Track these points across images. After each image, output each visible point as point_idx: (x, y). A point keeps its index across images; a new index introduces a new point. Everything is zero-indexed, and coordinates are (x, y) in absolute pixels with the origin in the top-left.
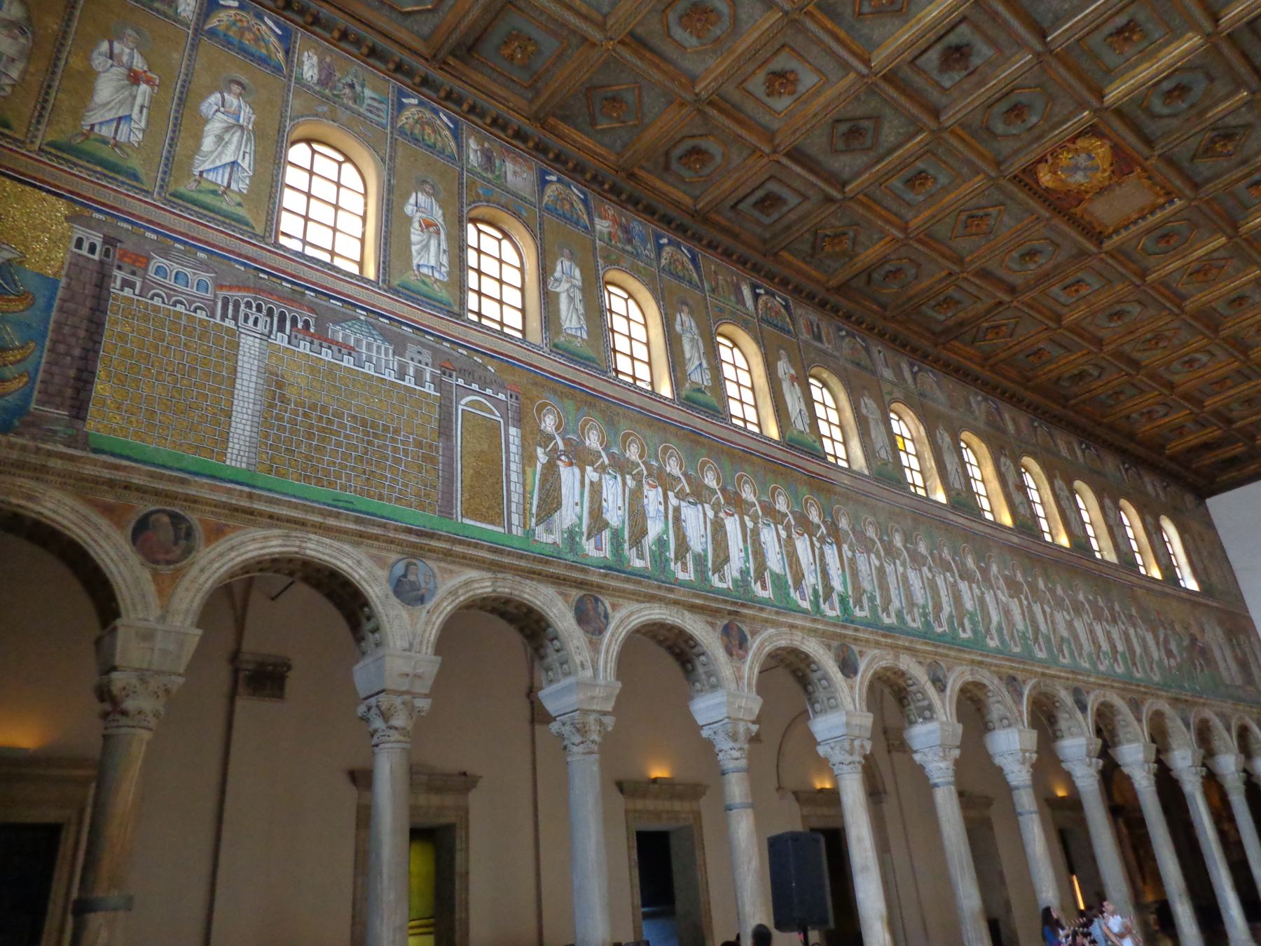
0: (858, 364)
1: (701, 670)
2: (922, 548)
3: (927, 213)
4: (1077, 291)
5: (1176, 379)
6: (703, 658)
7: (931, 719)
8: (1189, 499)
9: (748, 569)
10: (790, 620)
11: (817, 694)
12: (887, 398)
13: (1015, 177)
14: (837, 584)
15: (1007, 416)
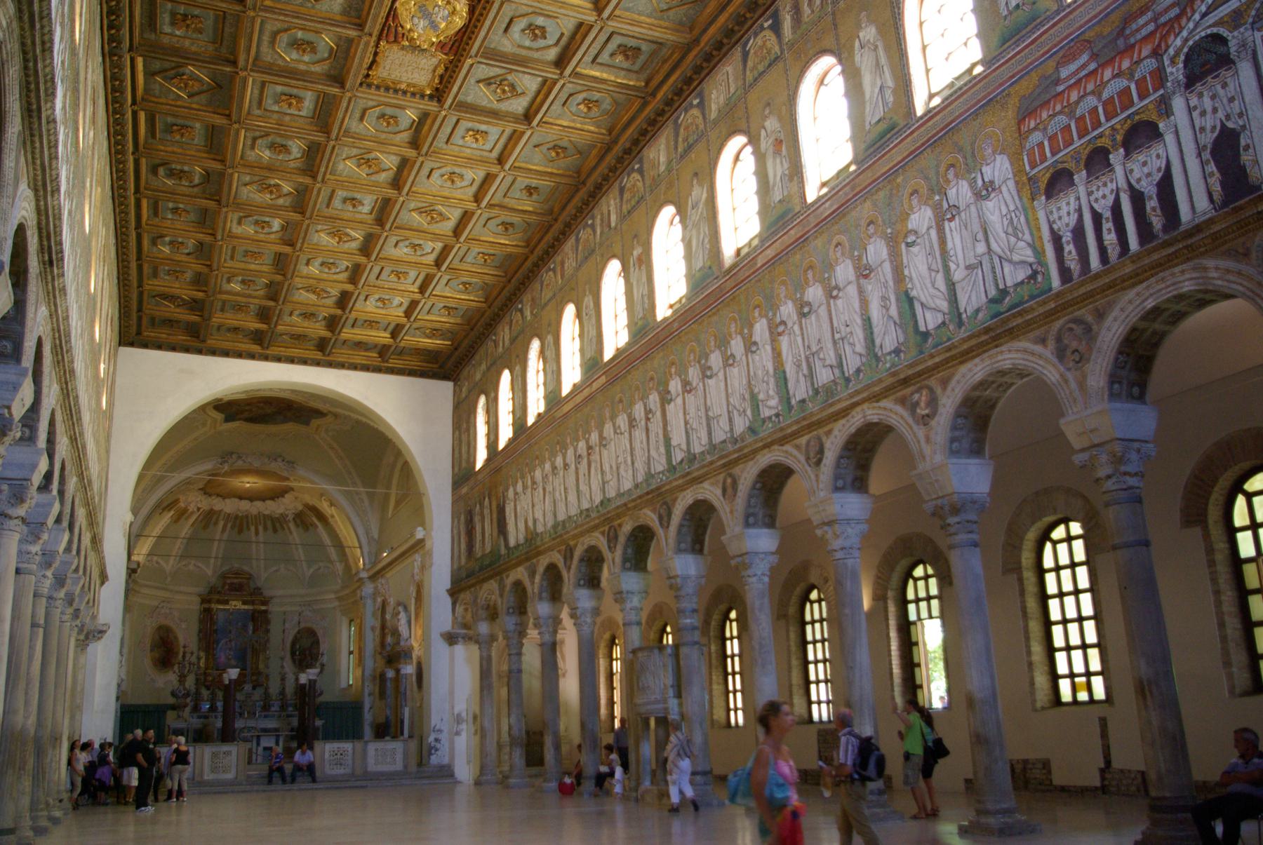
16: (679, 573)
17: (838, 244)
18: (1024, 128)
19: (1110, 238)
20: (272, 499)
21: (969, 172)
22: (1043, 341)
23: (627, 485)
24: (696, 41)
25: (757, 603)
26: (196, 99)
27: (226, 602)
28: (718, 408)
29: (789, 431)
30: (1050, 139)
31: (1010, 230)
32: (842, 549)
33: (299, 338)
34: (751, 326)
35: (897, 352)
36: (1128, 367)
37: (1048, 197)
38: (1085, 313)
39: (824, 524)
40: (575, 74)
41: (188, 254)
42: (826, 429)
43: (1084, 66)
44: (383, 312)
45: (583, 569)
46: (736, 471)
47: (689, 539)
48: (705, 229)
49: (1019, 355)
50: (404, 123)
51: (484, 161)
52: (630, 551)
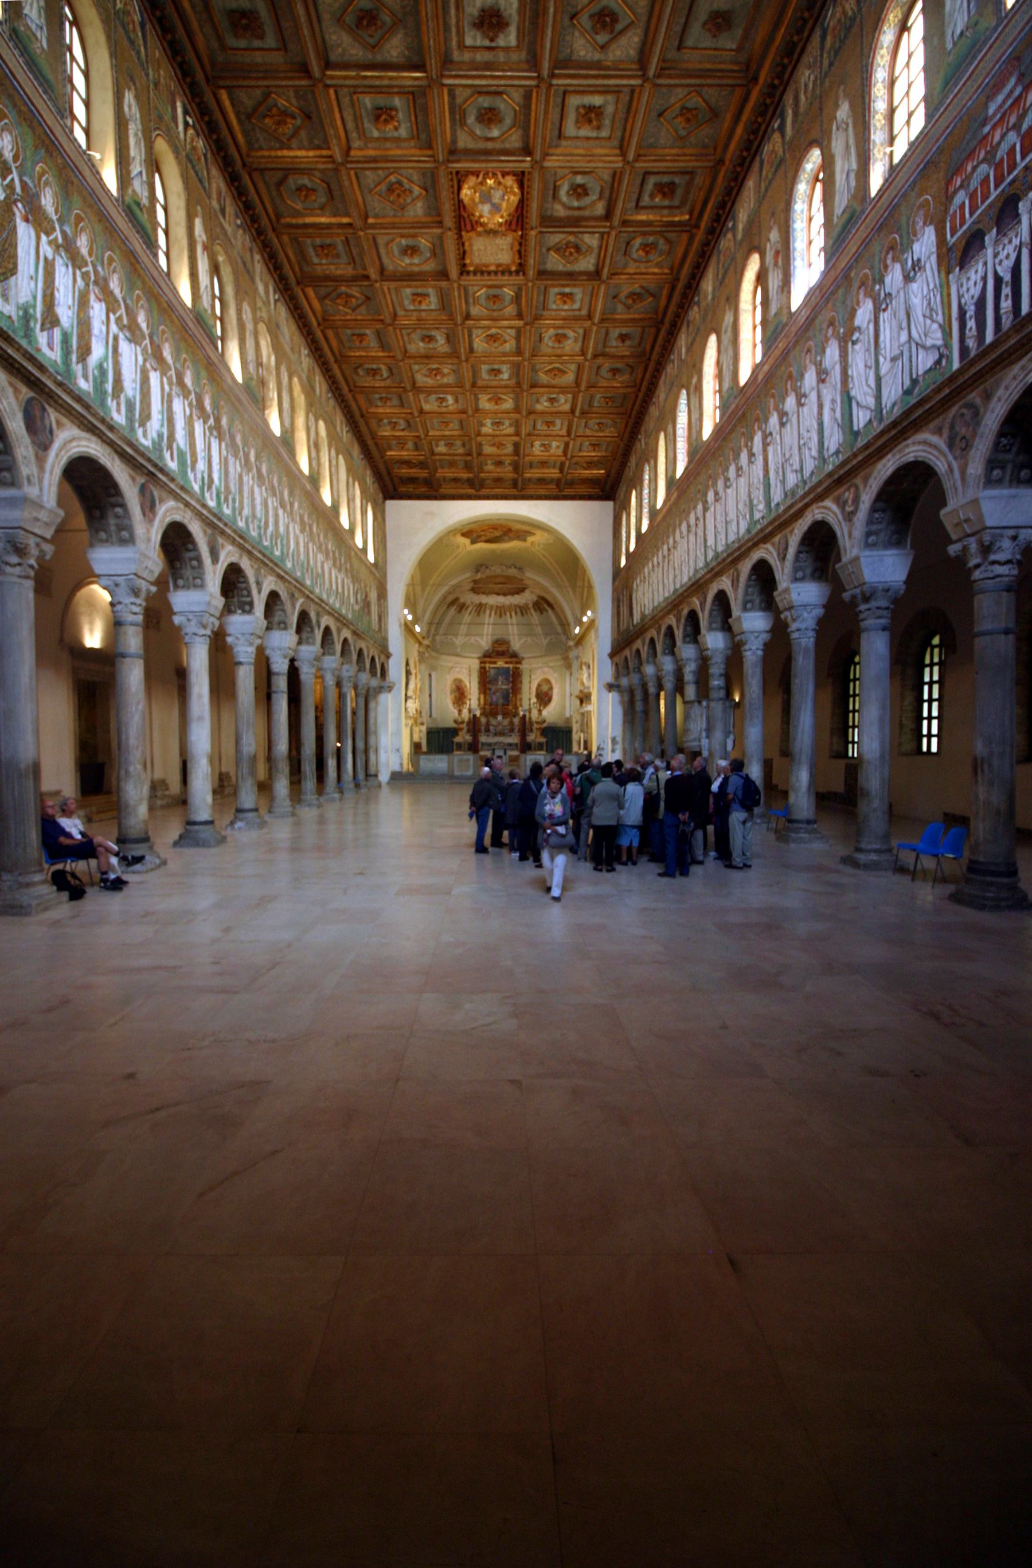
0: (244, 264)
1: (112, 521)
2: (264, 470)
3: (371, 153)
4: (420, 302)
5: (427, 407)
6: (119, 510)
7: (250, 612)
8: (381, 495)
9: (163, 434)
10: (188, 499)
11: (183, 572)
12: (259, 314)
13: (451, 173)
14: (216, 476)
15: (317, 378)
16: (709, 646)
17: (809, 350)
18: (951, 189)
19: (1006, 304)
20: (517, 593)
21: (903, 252)
22: (939, 431)
23: (685, 579)
24: (721, 162)
25: (750, 672)
26: (358, 311)
27: (495, 663)
28: (732, 516)
29: (767, 531)
30: (972, 197)
31: (928, 314)
32: (798, 630)
33: (498, 480)
34: (752, 439)
35: (837, 453)
36: (1015, 449)
37: (961, 270)
38: (974, 397)
39: (786, 609)
40: (625, 223)
41: (403, 430)
42: (791, 528)
43: (1011, 92)
44: (546, 454)
45: (667, 642)
46: (739, 566)
47: (719, 620)
48: (731, 352)
49: (921, 447)
50: (508, 299)
51: (576, 319)
52: (689, 628)
